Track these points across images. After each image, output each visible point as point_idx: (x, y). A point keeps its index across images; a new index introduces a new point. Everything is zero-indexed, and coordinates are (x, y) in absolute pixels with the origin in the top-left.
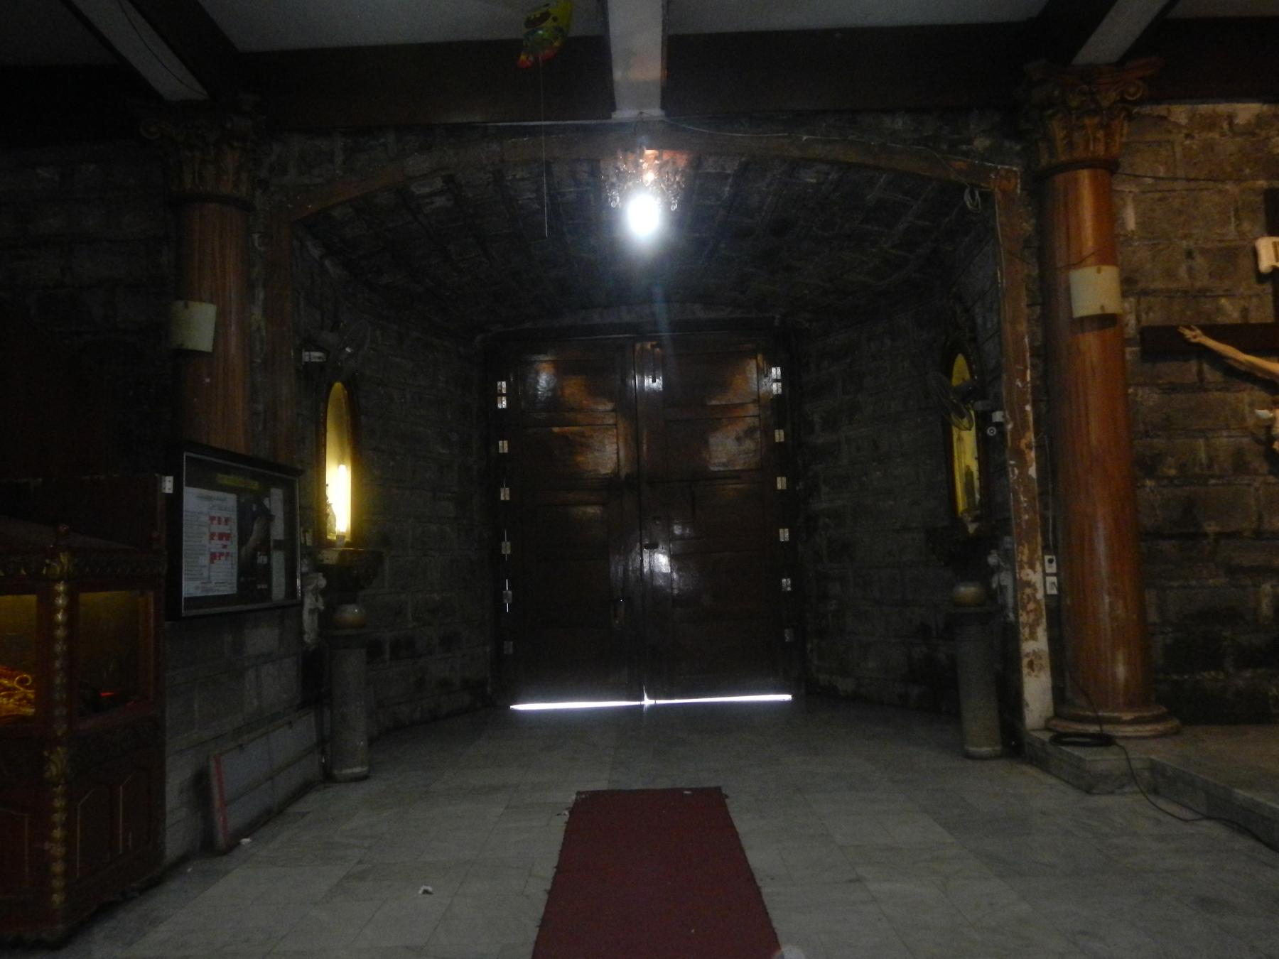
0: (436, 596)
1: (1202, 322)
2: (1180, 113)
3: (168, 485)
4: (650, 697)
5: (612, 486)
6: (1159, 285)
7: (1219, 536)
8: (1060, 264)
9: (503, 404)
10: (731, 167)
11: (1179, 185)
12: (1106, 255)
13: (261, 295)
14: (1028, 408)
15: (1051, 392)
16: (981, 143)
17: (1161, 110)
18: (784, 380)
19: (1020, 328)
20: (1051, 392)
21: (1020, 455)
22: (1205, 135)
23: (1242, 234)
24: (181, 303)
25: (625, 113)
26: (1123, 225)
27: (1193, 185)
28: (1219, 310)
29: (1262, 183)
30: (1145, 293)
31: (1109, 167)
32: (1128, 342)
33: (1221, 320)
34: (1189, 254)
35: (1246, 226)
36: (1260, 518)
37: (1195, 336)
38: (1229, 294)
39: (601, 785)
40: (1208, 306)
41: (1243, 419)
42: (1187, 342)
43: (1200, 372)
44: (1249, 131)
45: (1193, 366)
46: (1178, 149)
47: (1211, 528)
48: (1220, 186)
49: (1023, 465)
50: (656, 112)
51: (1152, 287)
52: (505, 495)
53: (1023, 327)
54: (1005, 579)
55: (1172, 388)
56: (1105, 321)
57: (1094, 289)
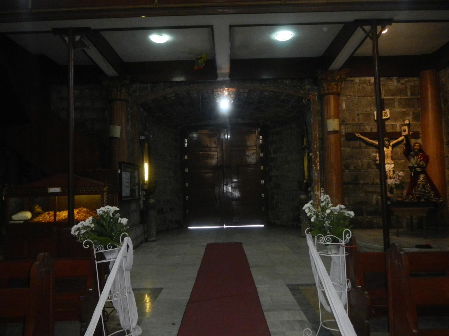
0: (168, 197)
1: (361, 131)
2: (357, 80)
3: (119, 171)
4: (226, 225)
5: (216, 168)
6: (350, 122)
7: (363, 184)
8: (326, 117)
9: (186, 145)
10: (247, 91)
11: (356, 98)
12: (337, 116)
13: (130, 123)
14: (318, 152)
15: (323, 148)
16: (308, 87)
17: (352, 79)
18: (263, 140)
19: (316, 133)
20: (323, 148)
21: (316, 164)
22: (363, 85)
23: (371, 110)
24: (112, 126)
25: (220, 79)
26: (342, 107)
27: (359, 98)
28: (365, 129)
30: (347, 124)
31: (338, 94)
32: (343, 136)
33: (366, 131)
34: (358, 115)
35: (373, 108)
36: (373, 180)
37: (358, 135)
38: (368, 125)
39: (213, 241)
40: (362, 127)
41: (370, 155)
42: (357, 137)
43: (360, 144)
45: (358, 142)
46: (356, 89)
47: (362, 182)
48: (366, 98)
49: (316, 166)
50: (228, 79)
51: (349, 123)
52: (187, 170)
53: (317, 132)
54: (312, 194)
55: (353, 148)
56: (335, 132)
57: (333, 124)
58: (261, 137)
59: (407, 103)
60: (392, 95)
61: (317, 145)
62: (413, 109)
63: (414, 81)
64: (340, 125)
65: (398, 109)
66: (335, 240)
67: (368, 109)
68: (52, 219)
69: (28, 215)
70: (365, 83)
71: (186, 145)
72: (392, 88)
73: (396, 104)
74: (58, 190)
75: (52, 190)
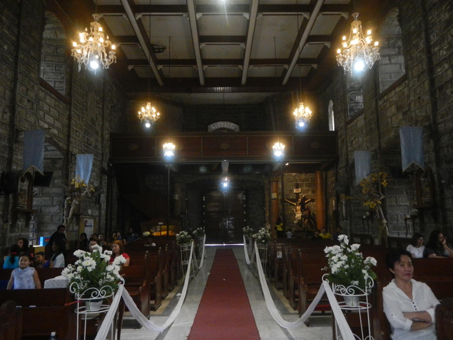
9: (204, 200)
12: (276, 192)
16: (264, 177)
18: (246, 197)
19: (267, 199)
20: (270, 206)
44: (294, 176)
47: (288, 222)
52: (204, 213)
56: (275, 199)
57: (274, 196)
58: (244, 196)
61: (267, 204)
64: (278, 195)
65: (305, 188)
67: (291, 188)
71: (204, 200)
74: (162, 223)
75: (160, 223)
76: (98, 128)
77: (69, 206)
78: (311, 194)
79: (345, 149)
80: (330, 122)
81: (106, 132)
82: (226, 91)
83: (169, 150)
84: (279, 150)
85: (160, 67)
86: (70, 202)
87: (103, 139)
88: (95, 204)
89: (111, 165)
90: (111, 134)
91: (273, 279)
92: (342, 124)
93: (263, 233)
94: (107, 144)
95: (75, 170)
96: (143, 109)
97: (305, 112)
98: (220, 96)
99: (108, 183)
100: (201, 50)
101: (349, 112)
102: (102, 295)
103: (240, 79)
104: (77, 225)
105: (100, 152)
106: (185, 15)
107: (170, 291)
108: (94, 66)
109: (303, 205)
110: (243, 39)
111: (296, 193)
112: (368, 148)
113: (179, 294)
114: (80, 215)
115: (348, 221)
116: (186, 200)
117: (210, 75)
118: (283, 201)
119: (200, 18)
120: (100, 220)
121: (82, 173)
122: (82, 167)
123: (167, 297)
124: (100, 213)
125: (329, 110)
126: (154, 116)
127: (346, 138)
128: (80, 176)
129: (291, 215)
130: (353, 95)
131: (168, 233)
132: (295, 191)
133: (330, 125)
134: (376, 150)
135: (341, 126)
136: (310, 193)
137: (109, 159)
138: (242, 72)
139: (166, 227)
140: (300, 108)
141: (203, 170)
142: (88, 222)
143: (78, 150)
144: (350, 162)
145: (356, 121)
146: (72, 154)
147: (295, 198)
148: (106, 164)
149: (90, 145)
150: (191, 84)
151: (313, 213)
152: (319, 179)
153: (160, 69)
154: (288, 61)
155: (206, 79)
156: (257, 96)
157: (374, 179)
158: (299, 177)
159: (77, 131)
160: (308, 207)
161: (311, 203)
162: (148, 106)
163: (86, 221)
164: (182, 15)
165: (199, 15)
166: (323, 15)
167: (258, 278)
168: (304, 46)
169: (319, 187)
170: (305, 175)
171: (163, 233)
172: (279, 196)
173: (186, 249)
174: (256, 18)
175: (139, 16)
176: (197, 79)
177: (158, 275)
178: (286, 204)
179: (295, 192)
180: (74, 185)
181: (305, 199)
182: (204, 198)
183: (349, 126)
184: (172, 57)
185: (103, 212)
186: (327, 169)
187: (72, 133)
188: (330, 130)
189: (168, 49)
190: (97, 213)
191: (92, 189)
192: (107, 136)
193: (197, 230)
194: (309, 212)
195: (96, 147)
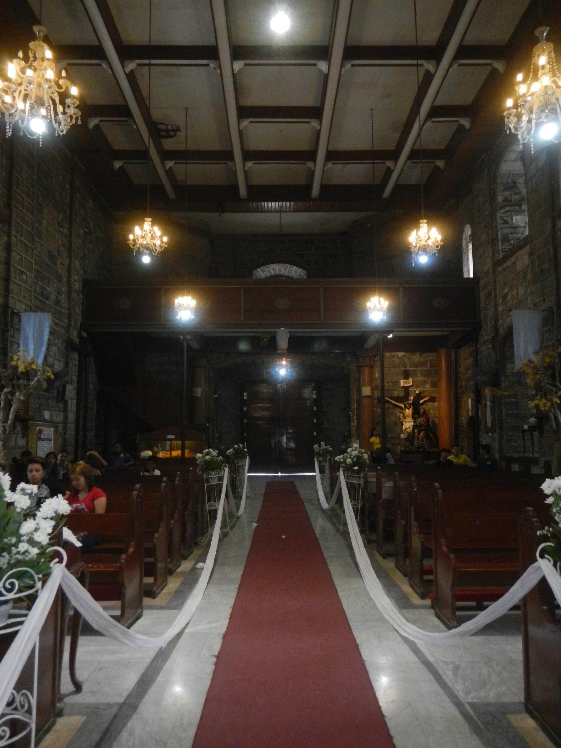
9: (246, 398)
12: (370, 384)
16: (349, 359)
18: (316, 394)
19: (354, 396)
20: (358, 409)
28: (394, 393)
29: (403, 368)
33: (394, 395)
34: (388, 382)
37: (387, 399)
38: (395, 390)
44: (401, 358)
47: (389, 436)
49: (354, 423)
50: (286, 352)
52: (245, 421)
53: (355, 396)
57: (366, 391)
58: (315, 392)
59: (428, 374)
60: (415, 367)
61: (355, 406)
62: (431, 378)
63: (429, 357)
64: (373, 390)
65: (419, 378)
66: (324, 459)
68: (168, 456)
69: (150, 453)
70: (394, 357)
71: (246, 398)
72: (416, 361)
73: (418, 374)
74: (173, 437)
75: (169, 437)
76: (61, 270)
77: (9, 404)
78: (430, 389)
79: (492, 309)
80: (465, 263)
81: (76, 277)
82: (284, 209)
83: (185, 308)
84: (377, 309)
85: (170, 164)
86: (10, 397)
87: (70, 287)
88: (57, 402)
89: (85, 335)
90: (85, 283)
91: (374, 537)
92: (488, 266)
93: (355, 453)
94: (78, 298)
95: (19, 340)
96: (137, 230)
97: (429, 238)
98: (274, 218)
99: (79, 365)
100: (240, 132)
101: (500, 243)
102: (9, 591)
103: (309, 187)
104: (23, 437)
105: (65, 311)
106: (212, 65)
107: (185, 558)
108: (38, 127)
109: (416, 406)
110: (316, 112)
111: (404, 387)
112: (535, 305)
113: (200, 565)
114: (29, 420)
115: (496, 435)
116: (216, 398)
117: (256, 181)
118: (382, 401)
119: (240, 71)
120: (65, 428)
121: (31, 346)
122: (30, 335)
123: (179, 570)
124: (66, 417)
125: (464, 243)
126: (158, 242)
127: (495, 289)
128: (26, 350)
129: (396, 424)
130: (508, 214)
131: (183, 453)
132: (402, 383)
133: (465, 269)
134: (551, 308)
135: (486, 269)
136: (428, 387)
137: (82, 325)
138: (313, 173)
139: (179, 442)
140: (421, 229)
141: (243, 346)
142: (44, 432)
143: (23, 307)
144: (502, 332)
145: (512, 260)
146: (13, 312)
147: (402, 394)
148: (75, 334)
149: (47, 299)
150: (224, 197)
151: (433, 422)
152: (443, 363)
153: (170, 168)
154: (394, 155)
155: (250, 188)
156: (337, 219)
157: (547, 360)
158: (409, 359)
159: (22, 273)
160: (424, 410)
161: (430, 403)
162: (147, 224)
163: (40, 431)
164: (208, 65)
165: (238, 65)
166: (460, 65)
167: (345, 535)
168: (424, 123)
169: (444, 376)
170: (421, 356)
171: (176, 453)
172: (376, 392)
173: (215, 482)
174: (340, 72)
175: (131, 66)
176: (236, 188)
177: (161, 530)
178: (387, 405)
179: (402, 385)
180: (16, 367)
181: (419, 397)
182: (246, 394)
183: (500, 269)
184: (191, 147)
185: (71, 416)
186: (458, 346)
187: (12, 275)
188: (466, 276)
189: (182, 134)
190: (59, 418)
191: (49, 374)
192: (76, 283)
193: (234, 449)
194: (428, 420)
195: (57, 302)
